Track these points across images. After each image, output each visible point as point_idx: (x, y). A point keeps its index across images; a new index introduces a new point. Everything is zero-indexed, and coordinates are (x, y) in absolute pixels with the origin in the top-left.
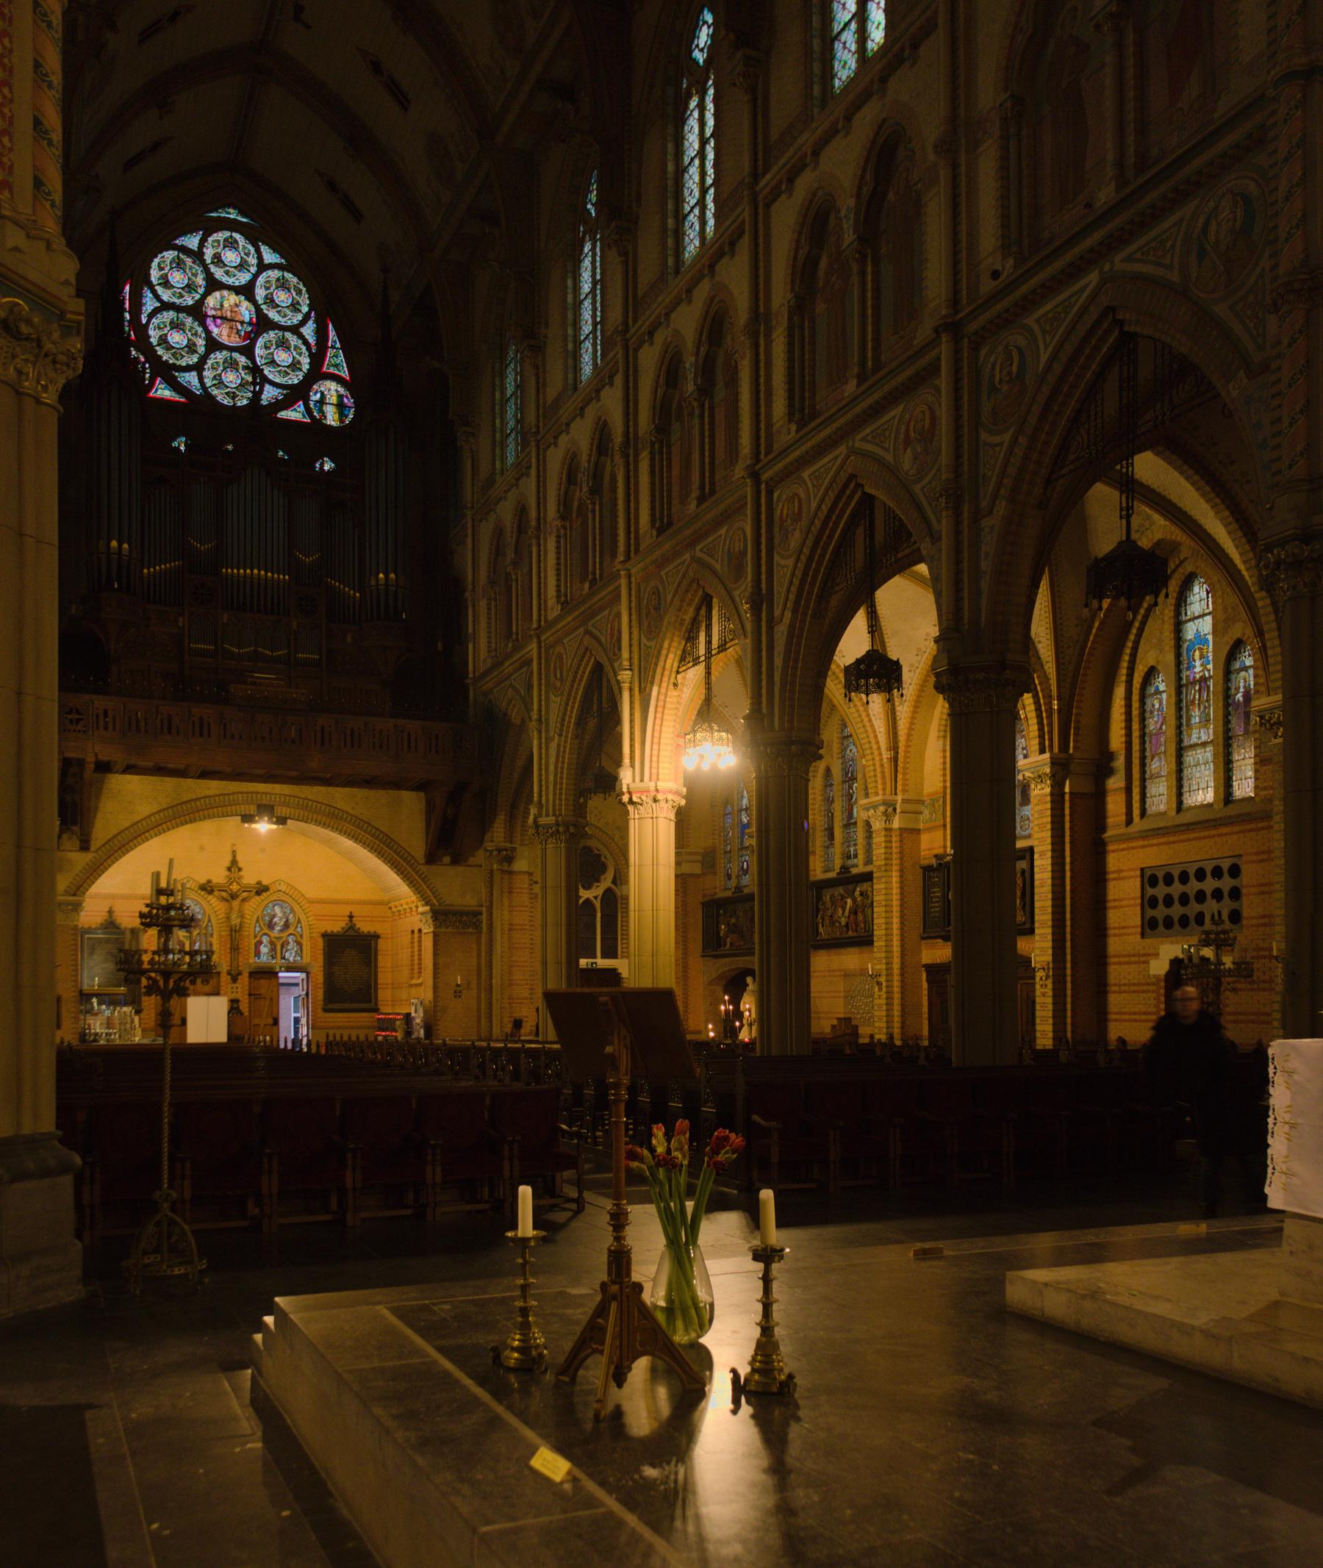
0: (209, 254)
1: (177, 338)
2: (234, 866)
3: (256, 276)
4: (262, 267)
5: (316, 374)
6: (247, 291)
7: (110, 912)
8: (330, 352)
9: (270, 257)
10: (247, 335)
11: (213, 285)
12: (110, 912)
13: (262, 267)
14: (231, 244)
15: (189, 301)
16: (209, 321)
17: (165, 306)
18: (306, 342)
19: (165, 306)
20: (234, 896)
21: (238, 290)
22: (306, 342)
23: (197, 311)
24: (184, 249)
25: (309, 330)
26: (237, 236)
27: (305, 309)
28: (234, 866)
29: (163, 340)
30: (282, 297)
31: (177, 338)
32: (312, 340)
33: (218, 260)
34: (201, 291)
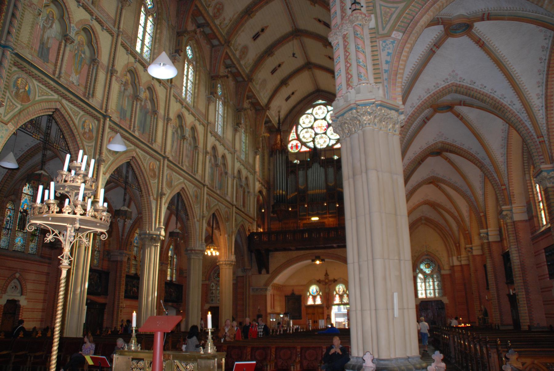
0: (314, 113)
1: (307, 135)
2: (327, 275)
4: (328, 112)
7: (293, 290)
11: (316, 120)
12: (293, 290)
14: (320, 109)
15: (310, 125)
16: (315, 129)
17: (304, 128)
19: (304, 128)
20: (326, 283)
21: (322, 119)
23: (312, 127)
24: (308, 114)
26: (322, 106)
28: (327, 275)
29: (304, 137)
31: (307, 135)
33: (317, 114)
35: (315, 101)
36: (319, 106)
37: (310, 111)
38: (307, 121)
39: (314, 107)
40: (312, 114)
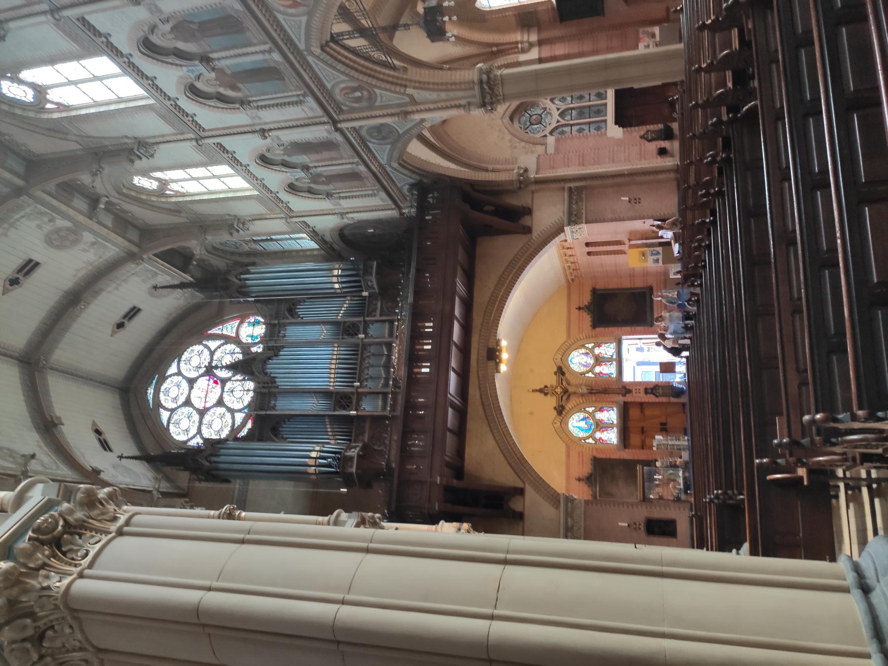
0: (172, 405)
3: (184, 377)
4: (179, 373)
5: (236, 340)
6: (191, 382)
8: (225, 332)
9: (173, 369)
10: (216, 382)
11: (188, 403)
13: (179, 373)
14: (167, 391)
18: (219, 347)
21: (191, 388)
22: (219, 347)
25: (213, 344)
26: (163, 388)
27: (201, 348)
30: (195, 361)
32: (218, 343)
33: (175, 399)
34: (191, 409)
35: (148, 401)
36: (162, 396)
37: (165, 415)
38: (184, 424)
39: (158, 405)
40: (172, 411)
